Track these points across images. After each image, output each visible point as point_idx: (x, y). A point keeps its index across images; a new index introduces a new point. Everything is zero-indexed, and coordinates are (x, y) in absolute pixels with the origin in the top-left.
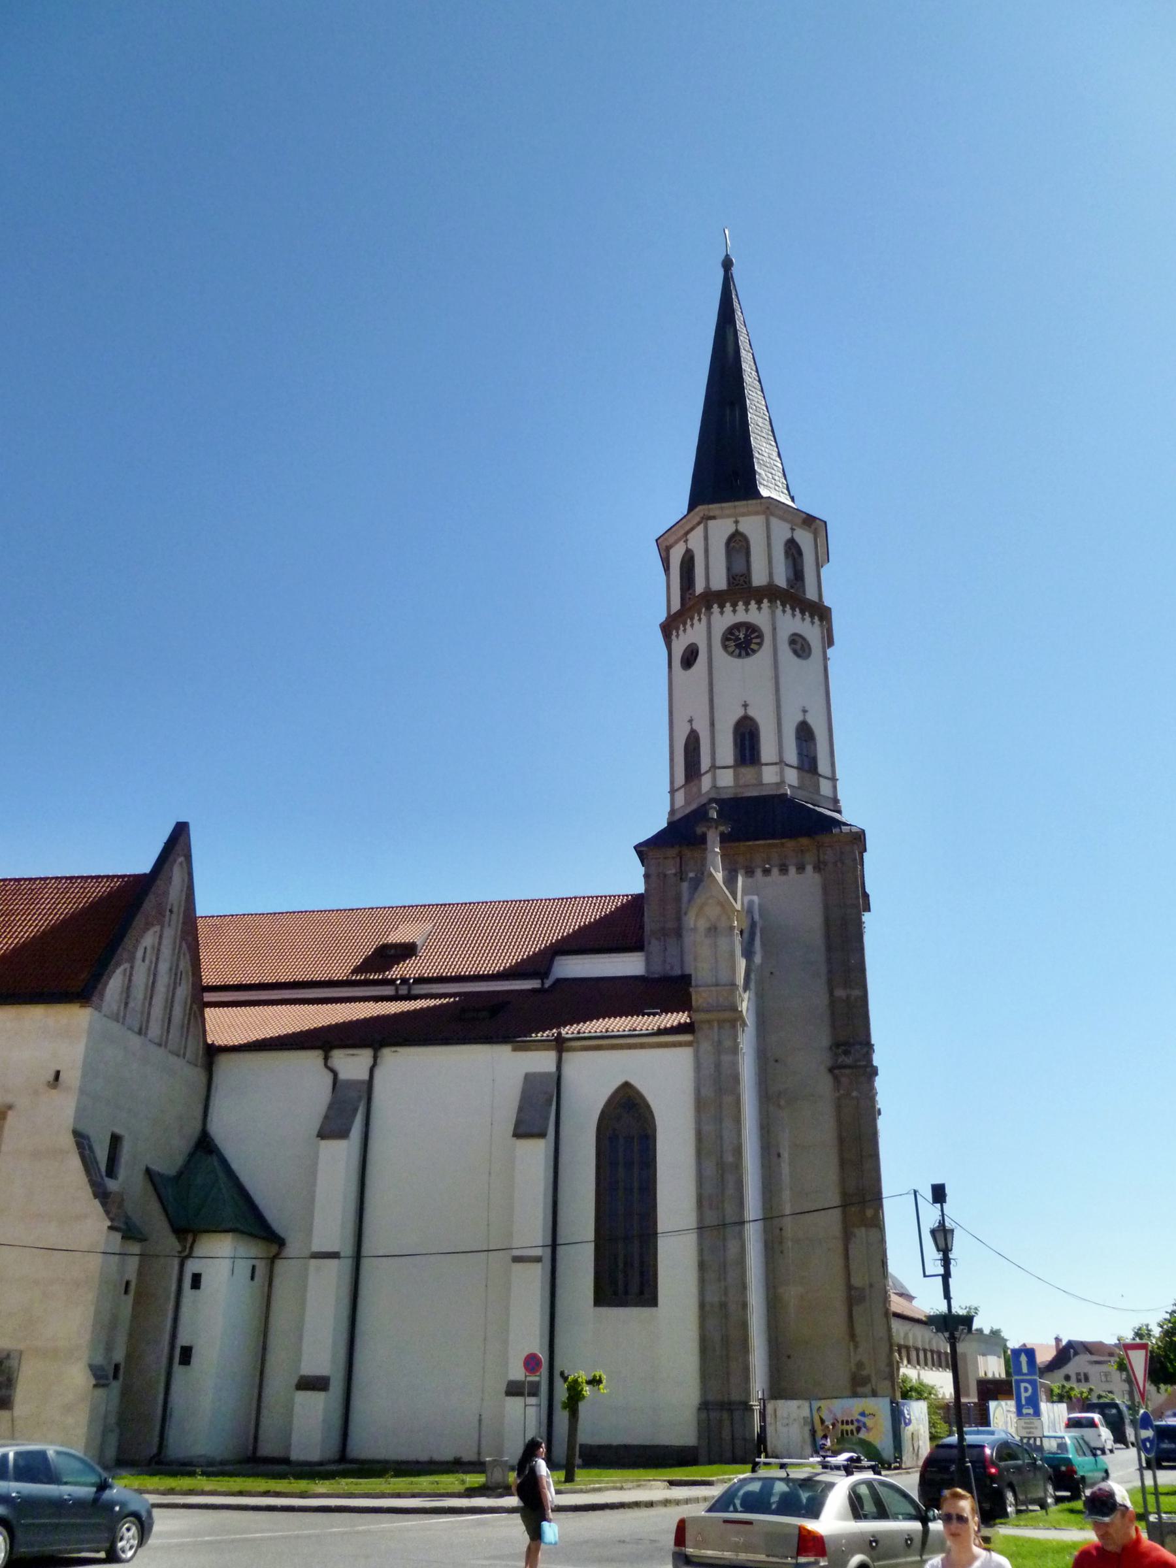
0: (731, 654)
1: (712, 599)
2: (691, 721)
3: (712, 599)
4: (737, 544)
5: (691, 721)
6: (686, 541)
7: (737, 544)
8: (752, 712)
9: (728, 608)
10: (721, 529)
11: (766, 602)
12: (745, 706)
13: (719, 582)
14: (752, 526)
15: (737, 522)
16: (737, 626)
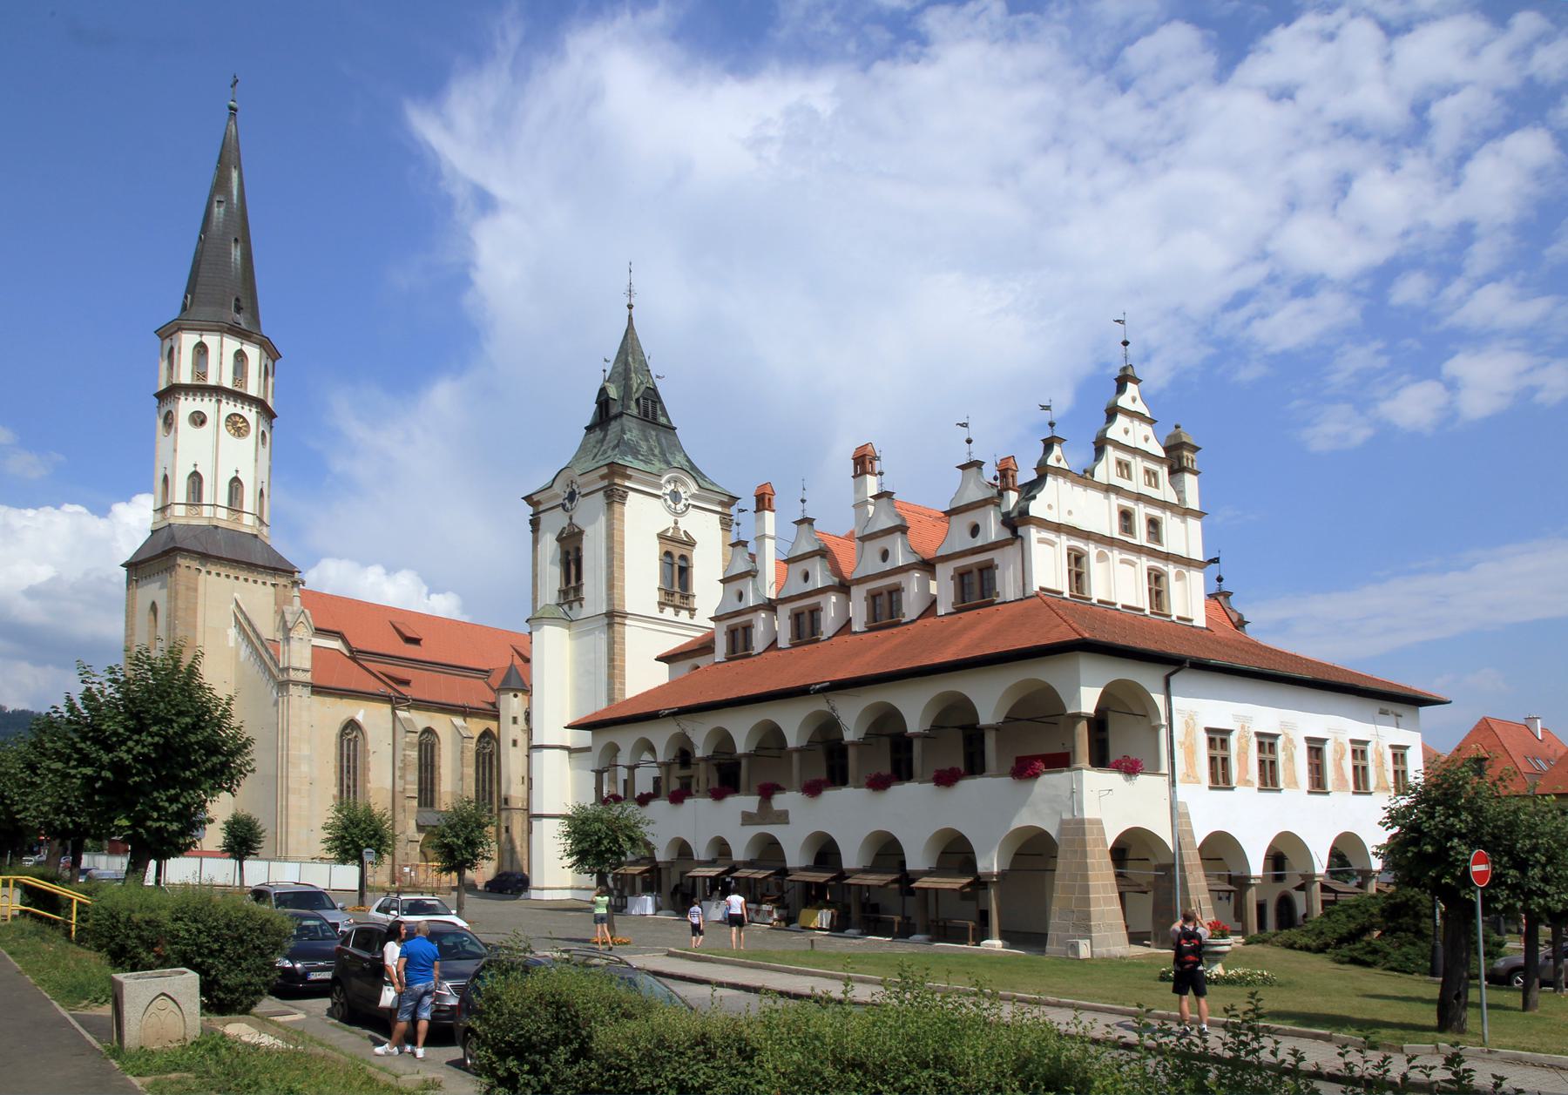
0: (229, 431)
1: (218, 391)
2: (195, 465)
3: (218, 391)
4: (240, 356)
5: (195, 465)
6: (201, 335)
7: (240, 356)
8: (239, 476)
9: (232, 403)
10: (232, 344)
11: (254, 410)
12: (237, 471)
13: (228, 383)
14: (253, 353)
15: (242, 343)
16: (235, 415)
